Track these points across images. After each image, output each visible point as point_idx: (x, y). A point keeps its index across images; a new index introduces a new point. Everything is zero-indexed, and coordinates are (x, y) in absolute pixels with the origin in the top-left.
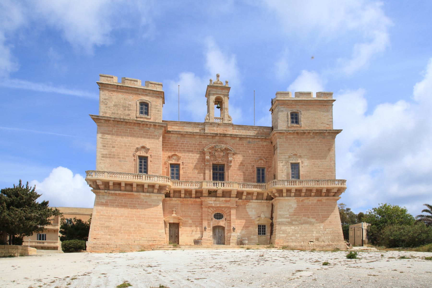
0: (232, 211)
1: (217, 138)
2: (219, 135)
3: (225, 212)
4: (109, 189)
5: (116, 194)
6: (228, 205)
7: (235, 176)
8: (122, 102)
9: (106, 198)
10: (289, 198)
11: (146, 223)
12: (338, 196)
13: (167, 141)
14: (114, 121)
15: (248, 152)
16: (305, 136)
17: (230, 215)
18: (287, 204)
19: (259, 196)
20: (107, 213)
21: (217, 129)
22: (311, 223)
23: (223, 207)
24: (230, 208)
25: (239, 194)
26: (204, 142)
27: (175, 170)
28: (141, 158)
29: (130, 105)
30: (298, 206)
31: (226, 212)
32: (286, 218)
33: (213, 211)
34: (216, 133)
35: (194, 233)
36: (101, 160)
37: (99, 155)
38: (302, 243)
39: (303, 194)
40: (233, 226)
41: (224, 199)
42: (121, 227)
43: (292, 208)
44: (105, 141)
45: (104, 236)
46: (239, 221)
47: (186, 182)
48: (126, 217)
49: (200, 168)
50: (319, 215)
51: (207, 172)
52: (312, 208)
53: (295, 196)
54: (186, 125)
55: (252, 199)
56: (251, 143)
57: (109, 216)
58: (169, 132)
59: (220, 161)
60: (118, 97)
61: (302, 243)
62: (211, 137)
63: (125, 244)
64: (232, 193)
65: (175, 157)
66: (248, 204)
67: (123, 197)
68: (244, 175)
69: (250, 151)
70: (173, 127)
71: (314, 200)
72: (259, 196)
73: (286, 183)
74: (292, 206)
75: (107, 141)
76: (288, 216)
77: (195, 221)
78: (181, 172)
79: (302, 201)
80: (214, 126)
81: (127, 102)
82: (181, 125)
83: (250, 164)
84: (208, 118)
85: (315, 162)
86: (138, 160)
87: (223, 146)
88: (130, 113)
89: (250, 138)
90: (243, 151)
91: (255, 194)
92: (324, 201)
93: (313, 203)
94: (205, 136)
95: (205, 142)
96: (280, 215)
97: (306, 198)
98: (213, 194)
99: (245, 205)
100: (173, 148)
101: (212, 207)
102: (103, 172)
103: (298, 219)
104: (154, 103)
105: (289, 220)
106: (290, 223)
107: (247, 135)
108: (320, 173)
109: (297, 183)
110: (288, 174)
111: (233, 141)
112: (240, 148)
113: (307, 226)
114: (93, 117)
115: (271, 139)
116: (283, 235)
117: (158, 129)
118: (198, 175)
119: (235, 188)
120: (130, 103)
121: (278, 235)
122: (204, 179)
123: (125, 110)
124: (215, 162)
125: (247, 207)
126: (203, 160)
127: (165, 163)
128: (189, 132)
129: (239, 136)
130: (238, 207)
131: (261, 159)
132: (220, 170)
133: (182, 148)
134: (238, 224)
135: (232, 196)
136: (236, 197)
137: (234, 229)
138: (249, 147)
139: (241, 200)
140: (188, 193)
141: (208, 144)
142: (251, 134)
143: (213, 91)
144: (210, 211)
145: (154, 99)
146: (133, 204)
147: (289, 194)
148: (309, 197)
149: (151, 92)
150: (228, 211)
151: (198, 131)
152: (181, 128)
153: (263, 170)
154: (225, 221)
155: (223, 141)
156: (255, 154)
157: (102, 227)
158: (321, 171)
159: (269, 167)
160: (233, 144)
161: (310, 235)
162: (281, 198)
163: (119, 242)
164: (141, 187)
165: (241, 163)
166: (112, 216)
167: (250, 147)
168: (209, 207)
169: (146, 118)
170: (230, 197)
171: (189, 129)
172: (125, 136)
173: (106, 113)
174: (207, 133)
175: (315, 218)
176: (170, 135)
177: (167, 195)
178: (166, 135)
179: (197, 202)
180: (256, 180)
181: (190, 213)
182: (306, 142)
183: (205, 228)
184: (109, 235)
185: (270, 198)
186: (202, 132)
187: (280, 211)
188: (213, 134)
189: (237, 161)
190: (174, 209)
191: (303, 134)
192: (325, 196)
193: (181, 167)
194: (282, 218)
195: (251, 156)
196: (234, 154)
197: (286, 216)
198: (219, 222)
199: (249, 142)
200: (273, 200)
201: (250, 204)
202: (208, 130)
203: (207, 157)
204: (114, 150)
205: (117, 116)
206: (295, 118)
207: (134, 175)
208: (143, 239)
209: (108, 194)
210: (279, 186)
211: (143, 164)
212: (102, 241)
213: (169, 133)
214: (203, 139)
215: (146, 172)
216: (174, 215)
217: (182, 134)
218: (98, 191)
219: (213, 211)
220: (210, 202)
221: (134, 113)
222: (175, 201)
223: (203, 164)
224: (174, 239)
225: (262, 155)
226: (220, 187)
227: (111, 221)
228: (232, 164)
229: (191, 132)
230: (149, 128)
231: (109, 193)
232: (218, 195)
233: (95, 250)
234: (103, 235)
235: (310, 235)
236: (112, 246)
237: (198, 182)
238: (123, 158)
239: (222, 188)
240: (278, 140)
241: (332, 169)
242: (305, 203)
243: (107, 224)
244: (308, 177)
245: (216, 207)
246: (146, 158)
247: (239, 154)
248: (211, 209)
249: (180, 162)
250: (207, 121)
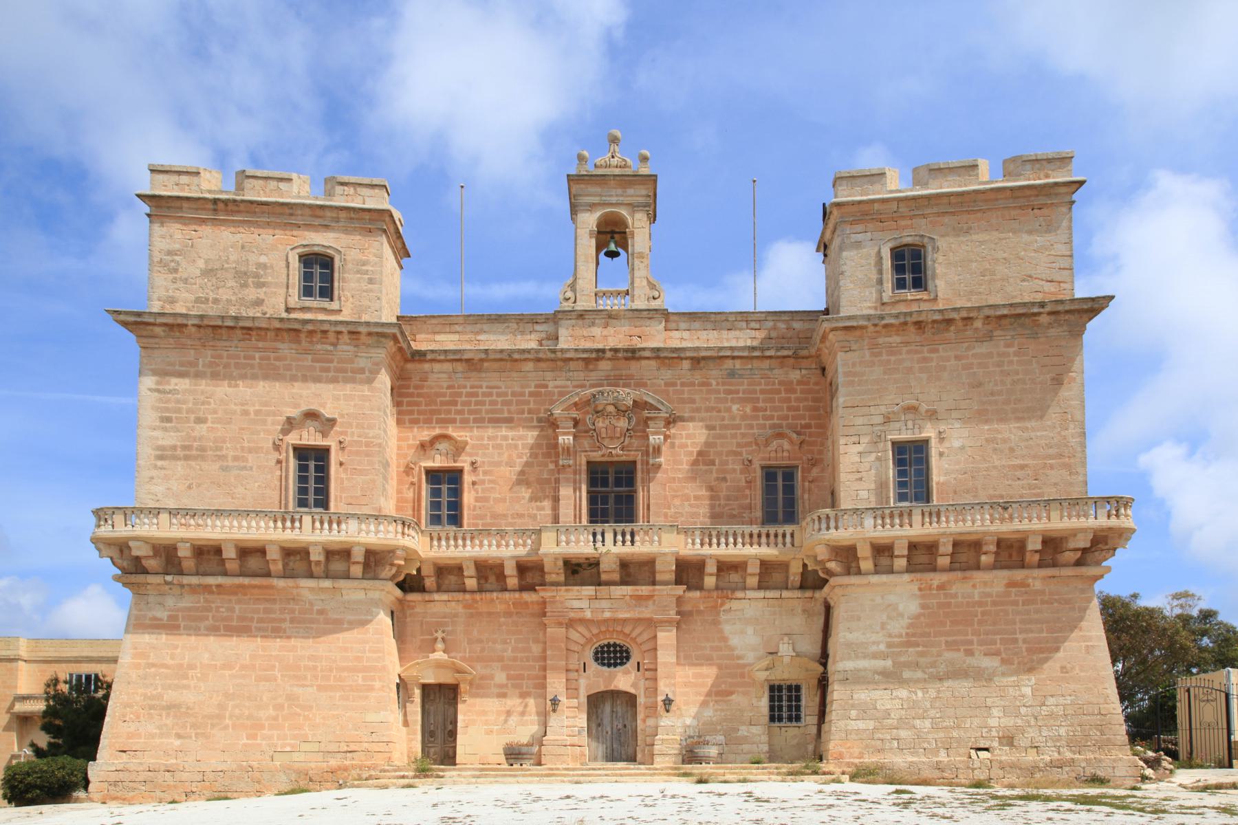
0: (660, 635)
1: (604, 365)
2: (609, 354)
3: (634, 640)
4: (181, 573)
5: (207, 588)
6: (646, 612)
7: (677, 502)
8: (232, 258)
9: (170, 602)
10: (884, 578)
11: (320, 688)
12: (1098, 563)
13: (417, 387)
14: (199, 326)
15: (729, 410)
16: (951, 335)
17: (655, 649)
18: (878, 600)
19: (770, 574)
20: (172, 658)
21: (605, 332)
22: (979, 675)
23: (625, 621)
24: (652, 624)
26: (554, 383)
27: (445, 493)
28: (302, 453)
29: (264, 266)
30: (923, 607)
31: (639, 640)
32: (875, 656)
33: (588, 635)
34: (600, 346)
35: (513, 720)
36: (155, 467)
37: (146, 452)
38: (942, 757)
39: (943, 561)
40: (667, 690)
41: (627, 590)
42: (221, 706)
43: (901, 615)
44: (168, 401)
45: (158, 741)
46: (690, 671)
47: (484, 532)
48: (243, 667)
49: (541, 482)
50: (1015, 641)
51: (566, 492)
52: (983, 613)
53: (911, 568)
54: (486, 327)
55: (744, 589)
56: (741, 376)
57: (181, 665)
58: (419, 356)
59: (615, 451)
60: (217, 242)
61: (943, 753)
62: (581, 363)
63: (234, 767)
64: (658, 567)
65: (443, 446)
66: (726, 607)
67: (234, 598)
68: (712, 498)
69: (735, 407)
70: (438, 337)
71: (990, 583)
72: (770, 574)
73: (869, 522)
74: (901, 607)
75: (178, 401)
76: (882, 647)
77: (521, 677)
78: (468, 498)
79: (941, 587)
80: (593, 324)
81: (253, 258)
82: (469, 328)
83: (736, 453)
84: (569, 294)
85: (998, 431)
86: (293, 463)
87: (627, 395)
88: (262, 296)
89: (734, 358)
90: (708, 410)
91: (754, 568)
92: (1038, 585)
93: (990, 595)
94: (555, 360)
95: (558, 383)
96: (849, 645)
97: (959, 574)
98: (586, 573)
99: (715, 609)
100: (439, 412)
101: (582, 621)
102: (156, 512)
103: (922, 660)
104: (353, 255)
105: (889, 663)
106: (891, 677)
107: (721, 349)
108: (1019, 473)
109: (917, 518)
110: (882, 486)
111: (667, 374)
112: (697, 397)
113: (962, 686)
114: (122, 317)
115: (818, 356)
116: (861, 725)
117: (368, 346)
118: (534, 504)
120: (263, 259)
121: (842, 724)
122: (556, 519)
123: (245, 285)
124: (597, 456)
125: (723, 617)
127: (408, 470)
128: (495, 351)
129: (689, 354)
130: (684, 618)
131: (780, 436)
132: (618, 483)
133: (470, 412)
134: (686, 685)
135: (659, 577)
136: (678, 582)
137: (668, 702)
138: (730, 392)
139: (697, 594)
140: (489, 572)
141: (567, 390)
142: (741, 344)
143: (592, 194)
144: (574, 635)
145: (356, 239)
146: (274, 620)
147: (884, 561)
148: (968, 574)
149: (343, 215)
150: (646, 636)
151: (533, 345)
152: (466, 337)
153: (789, 475)
154: (634, 673)
155: (630, 377)
156: (756, 418)
157: (152, 707)
158: (1022, 467)
159: (814, 463)
160: (667, 384)
161: (976, 722)
162: (854, 580)
163: (214, 762)
165: (700, 453)
166: (191, 667)
167: (737, 392)
168: (571, 624)
169: (324, 310)
170: (654, 583)
171: (498, 341)
172: (243, 377)
173: (172, 301)
174: (562, 350)
175: (997, 653)
176: (427, 366)
177: (410, 585)
178: (410, 366)
179: (526, 603)
180: (758, 514)
181: (499, 647)
182: (957, 358)
183: (555, 702)
184: (179, 736)
185: (812, 581)
186: (548, 345)
187: (850, 630)
188: (585, 351)
189: (684, 446)
190: (439, 635)
191: (944, 323)
192: (1040, 565)
193: (467, 478)
194: (857, 657)
195: (738, 427)
196: (670, 421)
197: (874, 648)
198: (611, 678)
199: (732, 374)
200: (826, 589)
201: (735, 605)
202: (569, 339)
203: (566, 439)
204: (201, 429)
205: (212, 310)
207: (283, 517)
208: (305, 747)
209: (177, 590)
210: (843, 534)
211: (313, 472)
212: (149, 760)
213: (420, 361)
214: (549, 375)
215: (323, 503)
216: (439, 655)
217: (468, 361)
218: (140, 578)
219: (588, 635)
220: (576, 604)
221: (280, 295)
222: (440, 604)
223: (552, 466)
224: (440, 747)
225: (786, 418)
227: (186, 687)
228: (662, 460)
229: (502, 351)
230: (335, 345)
231: (182, 586)
232: (604, 577)
233: (121, 792)
234: (153, 736)
235: (976, 722)
236: (185, 776)
237: (524, 532)
238: (236, 458)
239: (619, 549)
240: (840, 356)
241: (1072, 457)
242: (955, 596)
243: (170, 696)
244: (968, 492)
245: (599, 623)
246: (322, 455)
247: (692, 419)
248: (581, 629)
249: (464, 462)
250: (567, 306)
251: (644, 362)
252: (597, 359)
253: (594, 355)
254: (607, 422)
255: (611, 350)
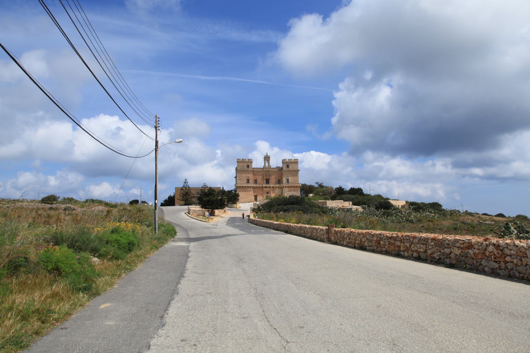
19: (279, 188)
25: (273, 187)
27: (256, 181)
72: (279, 188)
119: (272, 185)
126: (263, 178)
140: (259, 187)
164: (248, 187)
185: (281, 188)
206: (288, 166)
211: (248, 181)
221: (246, 168)
222: (256, 189)
226: (268, 186)
241: (298, 180)
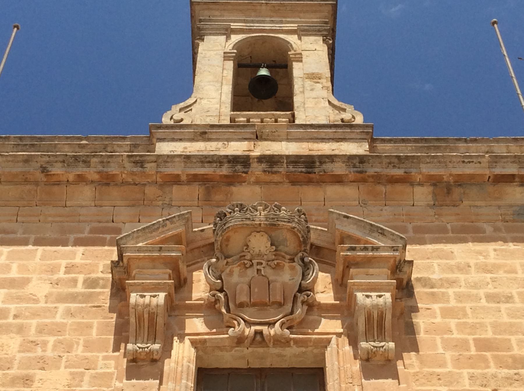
62: (197, 190)
214: (124, 213)
251: (332, 191)
252: (231, 180)
253: (225, 170)
254: (251, 273)
255: (261, 159)
